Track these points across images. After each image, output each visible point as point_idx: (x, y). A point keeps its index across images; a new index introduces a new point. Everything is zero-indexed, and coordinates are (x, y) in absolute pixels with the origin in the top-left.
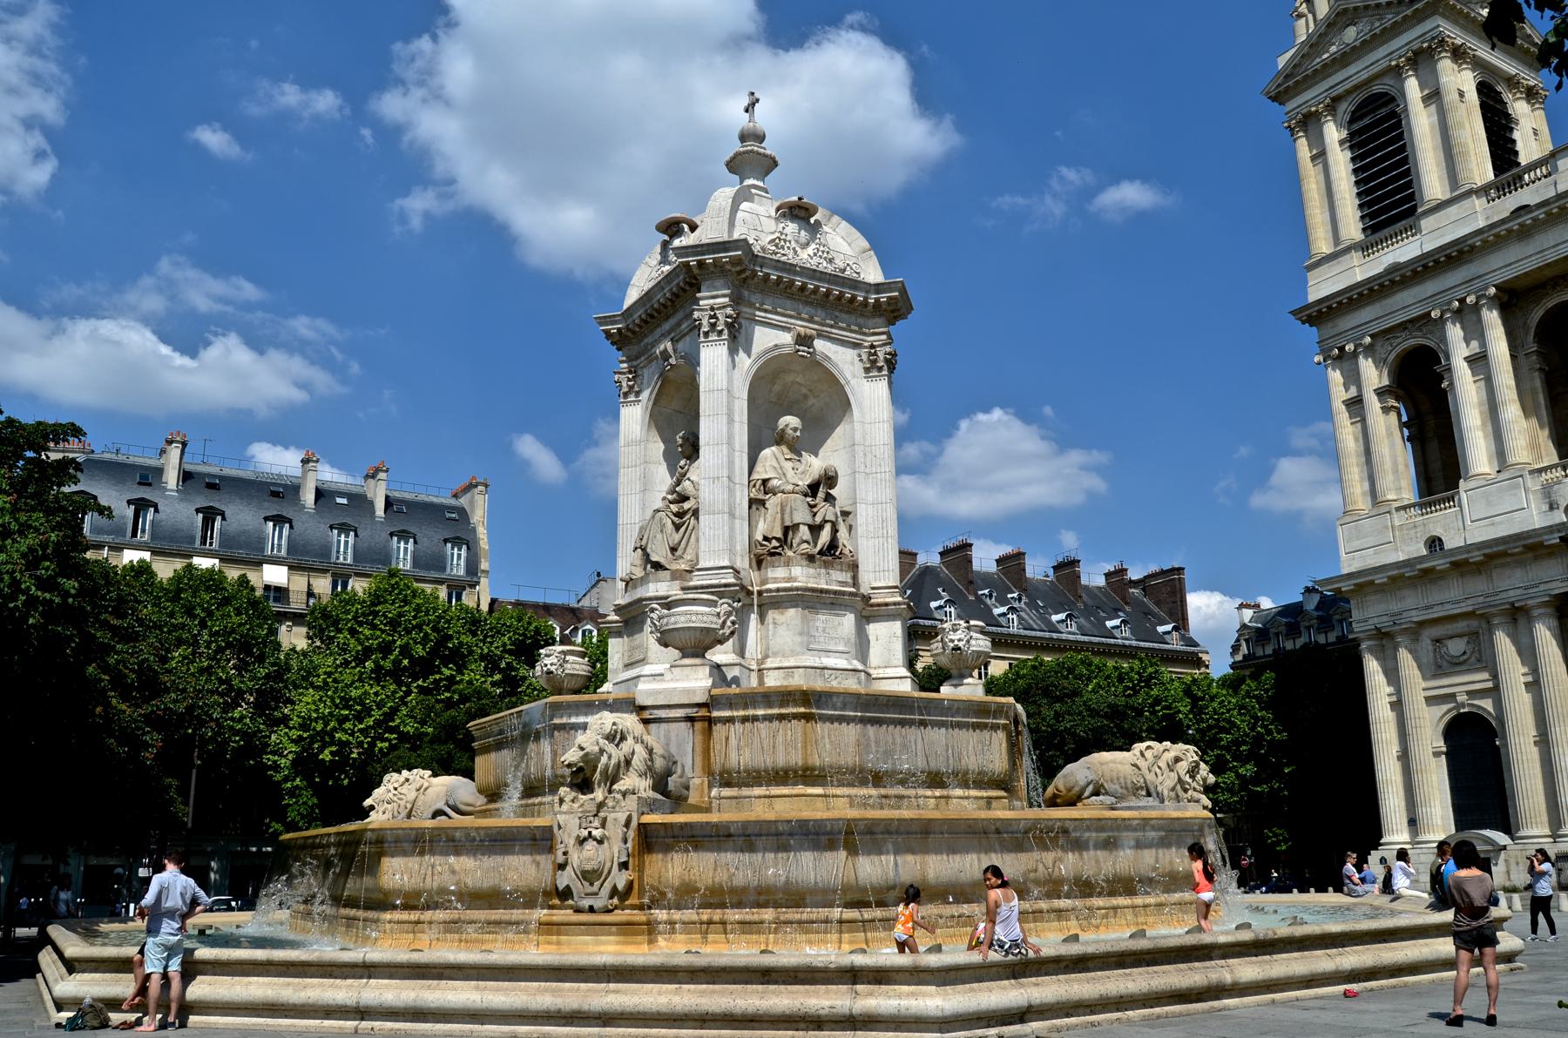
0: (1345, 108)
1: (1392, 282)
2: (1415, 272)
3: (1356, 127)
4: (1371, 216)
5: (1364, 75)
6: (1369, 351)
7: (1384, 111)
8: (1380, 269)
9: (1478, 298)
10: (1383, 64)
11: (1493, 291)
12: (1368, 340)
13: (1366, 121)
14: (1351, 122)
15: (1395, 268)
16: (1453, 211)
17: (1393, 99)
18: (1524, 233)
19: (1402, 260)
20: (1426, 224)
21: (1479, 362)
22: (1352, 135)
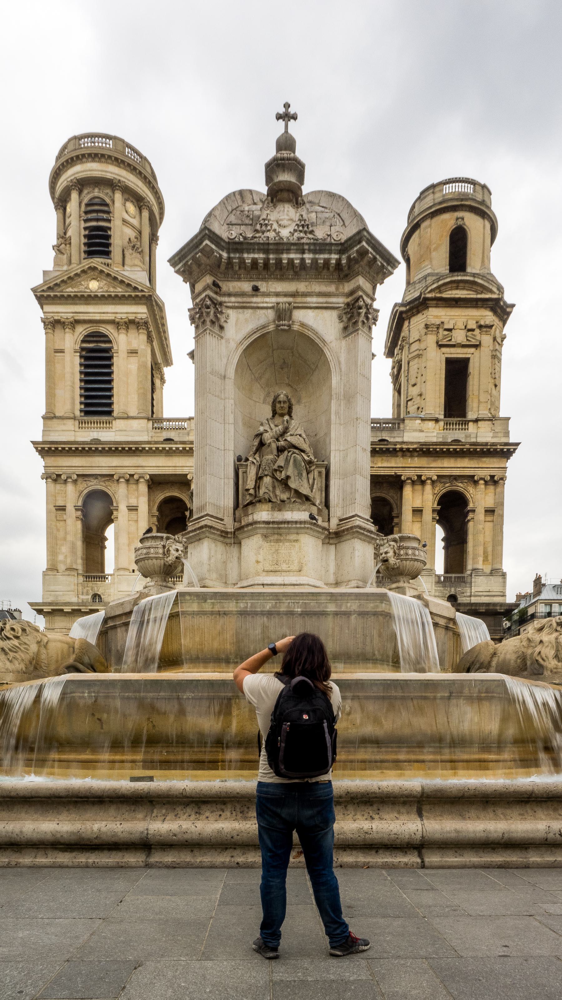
0: (81, 331)
1: (97, 449)
2: (110, 449)
3: (85, 345)
4: (87, 405)
5: (97, 317)
6: (75, 482)
7: (103, 345)
8: (88, 439)
9: (140, 477)
10: (111, 317)
11: (148, 477)
12: (75, 477)
13: (91, 345)
14: (83, 341)
15: (97, 441)
16: (135, 424)
17: (110, 342)
18: (169, 453)
19: (103, 439)
20: (118, 424)
21: (133, 509)
22: (82, 349)
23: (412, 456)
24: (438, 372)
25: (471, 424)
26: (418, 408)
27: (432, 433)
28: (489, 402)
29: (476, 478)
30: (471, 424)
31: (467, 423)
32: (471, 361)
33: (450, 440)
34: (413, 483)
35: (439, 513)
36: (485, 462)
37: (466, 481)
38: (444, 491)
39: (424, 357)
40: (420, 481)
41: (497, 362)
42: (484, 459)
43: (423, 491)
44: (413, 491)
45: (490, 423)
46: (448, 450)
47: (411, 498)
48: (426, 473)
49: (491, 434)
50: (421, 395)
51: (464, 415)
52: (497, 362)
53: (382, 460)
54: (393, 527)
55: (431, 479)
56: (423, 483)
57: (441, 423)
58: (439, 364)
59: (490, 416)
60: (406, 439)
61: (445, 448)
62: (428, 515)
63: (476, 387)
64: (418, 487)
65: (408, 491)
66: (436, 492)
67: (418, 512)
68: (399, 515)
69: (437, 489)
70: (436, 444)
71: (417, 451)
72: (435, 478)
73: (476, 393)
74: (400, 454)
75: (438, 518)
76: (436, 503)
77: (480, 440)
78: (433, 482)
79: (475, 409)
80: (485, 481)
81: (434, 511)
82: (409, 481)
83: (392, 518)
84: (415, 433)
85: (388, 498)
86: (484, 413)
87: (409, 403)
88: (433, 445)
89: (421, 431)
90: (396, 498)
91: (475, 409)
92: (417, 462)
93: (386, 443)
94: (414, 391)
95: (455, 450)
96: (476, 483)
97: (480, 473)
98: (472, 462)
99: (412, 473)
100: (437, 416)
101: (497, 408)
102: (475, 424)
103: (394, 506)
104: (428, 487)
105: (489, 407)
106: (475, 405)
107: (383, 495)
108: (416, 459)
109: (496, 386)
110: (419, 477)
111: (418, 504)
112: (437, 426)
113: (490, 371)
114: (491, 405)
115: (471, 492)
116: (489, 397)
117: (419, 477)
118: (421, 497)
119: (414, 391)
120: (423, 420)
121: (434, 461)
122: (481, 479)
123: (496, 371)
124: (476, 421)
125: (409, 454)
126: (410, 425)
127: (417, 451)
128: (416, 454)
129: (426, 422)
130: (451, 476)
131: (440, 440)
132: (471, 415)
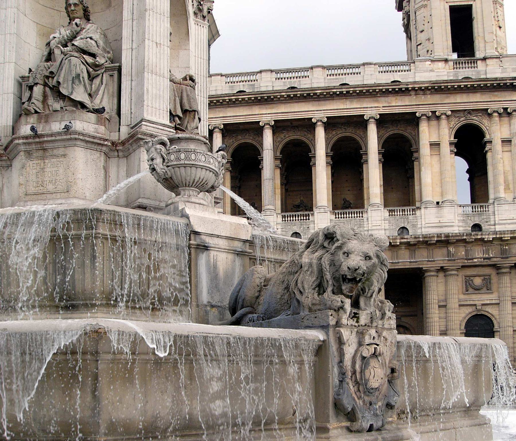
23: (424, 94)
24: (443, 18)
25: (479, 62)
26: (428, 51)
27: (443, 73)
28: (495, 42)
29: (489, 111)
30: (479, 62)
31: (475, 61)
32: (474, 7)
33: (460, 78)
34: (429, 118)
35: (456, 145)
36: (496, 96)
37: (481, 114)
38: (459, 125)
39: (428, 6)
40: (435, 117)
41: (498, 7)
42: (496, 93)
43: (439, 125)
44: (429, 126)
45: (497, 60)
46: (459, 86)
47: (427, 133)
48: (440, 109)
49: (500, 70)
50: (429, 39)
51: (473, 55)
52: (498, 7)
53: (396, 99)
54: (413, 161)
55: (445, 114)
56: (438, 118)
57: (451, 63)
58: (443, 11)
59: (497, 54)
60: (417, 79)
61: (456, 85)
62: (446, 149)
63: (481, 30)
64: (434, 123)
65: (424, 127)
66: (451, 126)
67: (435, 145)
68: (417, 151)
69: (453, 123)
70: (447, 82)
71: (430, 90)
72: (449, 113)
73: (481, 34)
74: (413, 93)
75: (456, 150)
76: (453, 136)
77: (489, 76)
78: (448, 116)
79: (482, 49)
80: (499, 113)
81: (451, 144)
82: (424, 117)
83: (412, 153)
84: (425, 73)
85: (406, 134)
86: (491, 52)
87: (419, 47)
88: (443, 83)
89: (432, 71)
90: (414, 134)
91: (482, 49)
92: (430, 99)
93: (398, 83)
94: (421, 37)
95: (466, 86)
96: (490, 115)
97: (492, 107)
98: (484, 97)
99: (426, 110)
100: (446, 57)
101: (504, 48)
102: (484, 62)
103: (413, 142)
104: (444, 122)
105: (495, 46)
106: (482, 45)
107: (401, 132)
108: (429, 96)
109: (500, 27)
110: (434, 112)
111: (434, 139)
112: (447, 66)
113: (493, 15)
114: (497, 44)
115: (486, 124)
116: (495, 38)
117: (434, 112)
118: (437, 132)
119: (421, 37)
120: (432, 61)
121: (447, 97)
122: (494, 112)
123: (499, 14)
124: (484, 59)
125: (421, 92)
126: (420, 66)
127: (430, 90)
128: (428, 92)
129: (436, 63)
130: (466, 110)
131: (452, 78)
132: (479, 55)
